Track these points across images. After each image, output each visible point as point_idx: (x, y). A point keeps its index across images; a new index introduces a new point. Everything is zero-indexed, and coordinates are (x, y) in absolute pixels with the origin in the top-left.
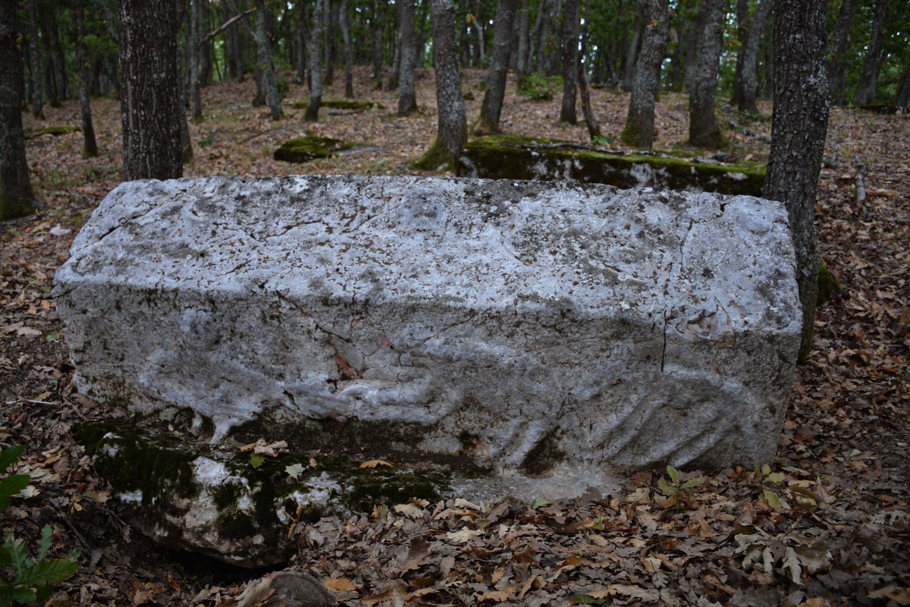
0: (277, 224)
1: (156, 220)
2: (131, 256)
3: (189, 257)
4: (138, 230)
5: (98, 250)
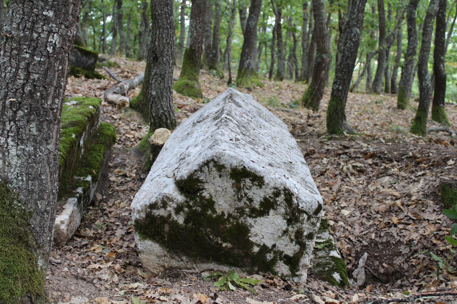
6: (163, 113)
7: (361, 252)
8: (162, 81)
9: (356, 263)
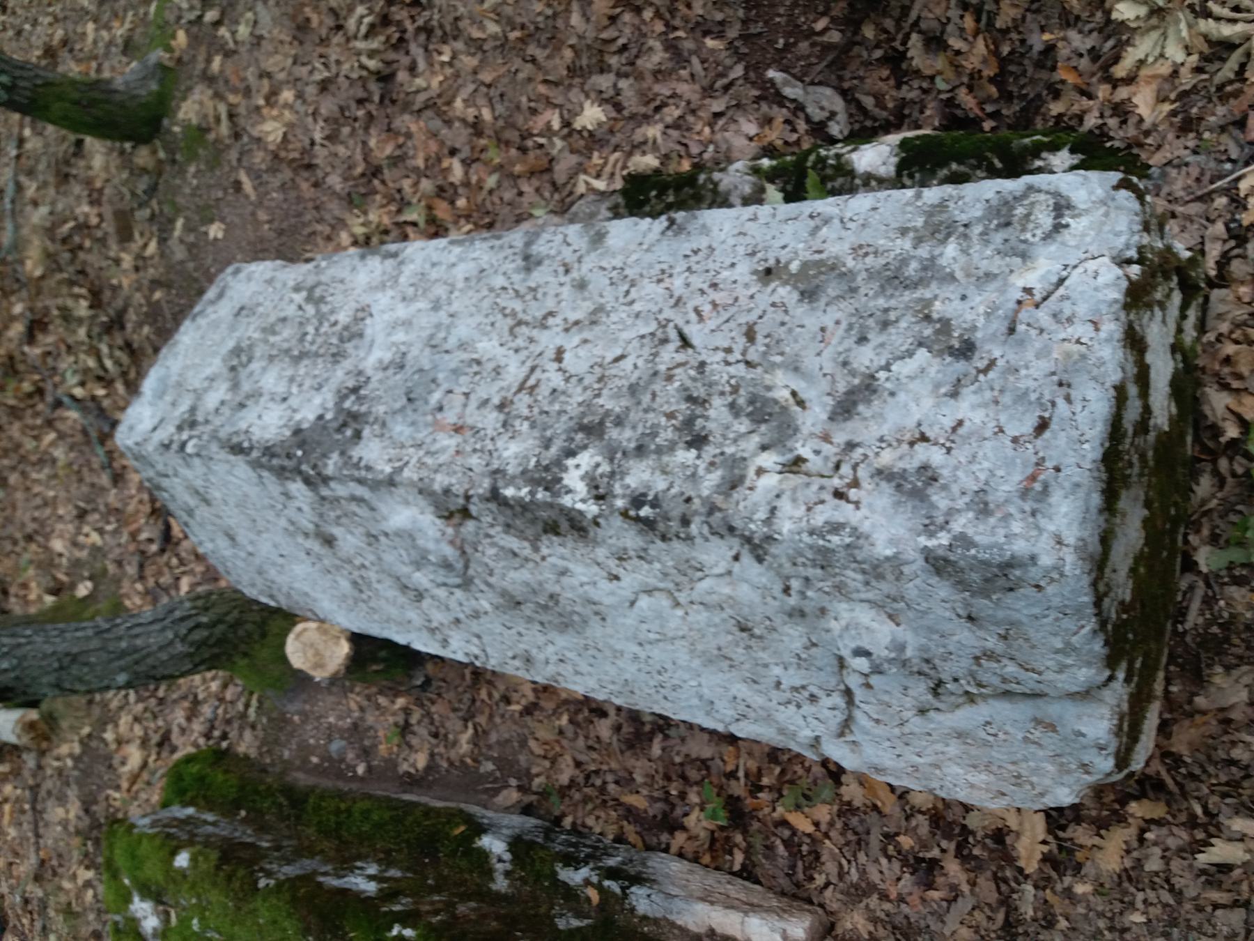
0: (636, 366)
1: (887, 368)
2: (924, 251)
3: (794, 267)
4: (928, 331)
5: (1018, 260)
6: (183, 640)
7: (764, 89)
8: (82, 659)
9: (792, 106)
